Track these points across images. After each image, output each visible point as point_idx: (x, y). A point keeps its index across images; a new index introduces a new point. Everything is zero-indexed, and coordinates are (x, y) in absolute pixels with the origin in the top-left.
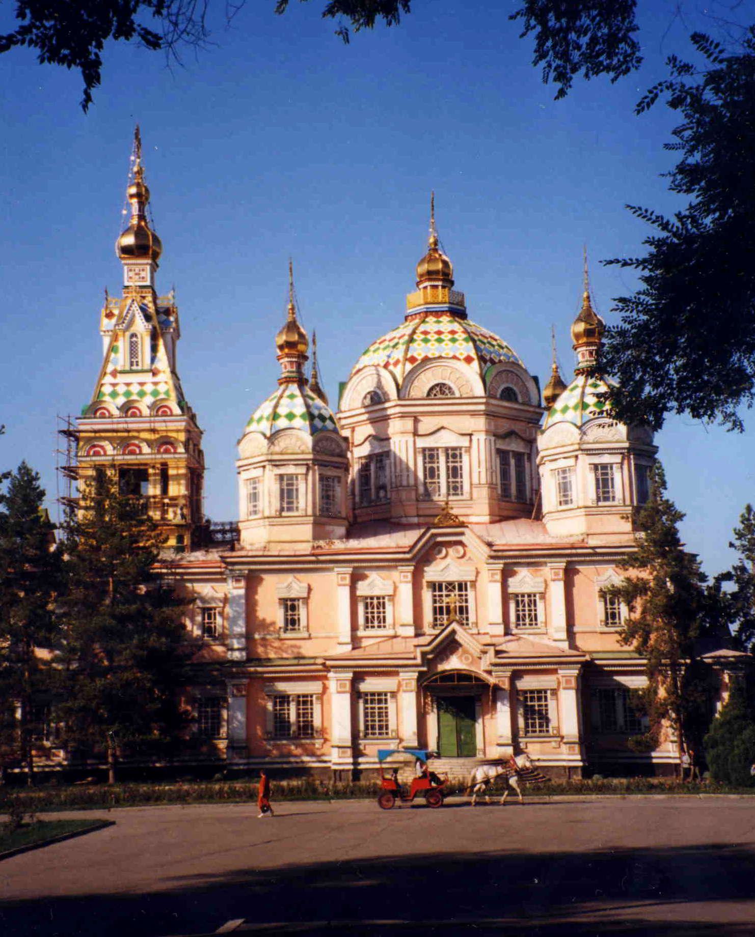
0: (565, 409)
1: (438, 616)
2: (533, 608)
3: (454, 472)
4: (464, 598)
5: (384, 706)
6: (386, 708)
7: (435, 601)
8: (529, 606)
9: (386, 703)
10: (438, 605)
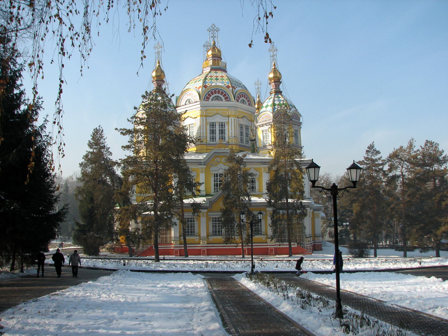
0: (267, 106)
1: (216, 187)
3: (222, 132)
5: (193, 223)
6: (194, 224)
9: (194, 222)
10: (216, 183)
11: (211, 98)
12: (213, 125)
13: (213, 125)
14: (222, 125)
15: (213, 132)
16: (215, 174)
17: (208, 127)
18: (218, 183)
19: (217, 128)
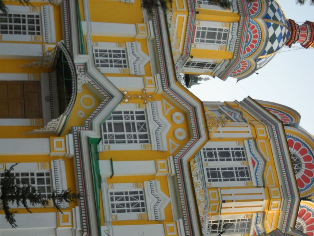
2: (131, 208)
3: (228, 174)
4: (133, 139)
7: (126, 112)
8: (133, 204)
9: (30, 33)
10: (123, 115)
11: (292, 150)
12: (240, 154)
14: (244, 174)
15: (225, 154)
16: (143, 112)
17: (233, 145)
19: (234, 164)
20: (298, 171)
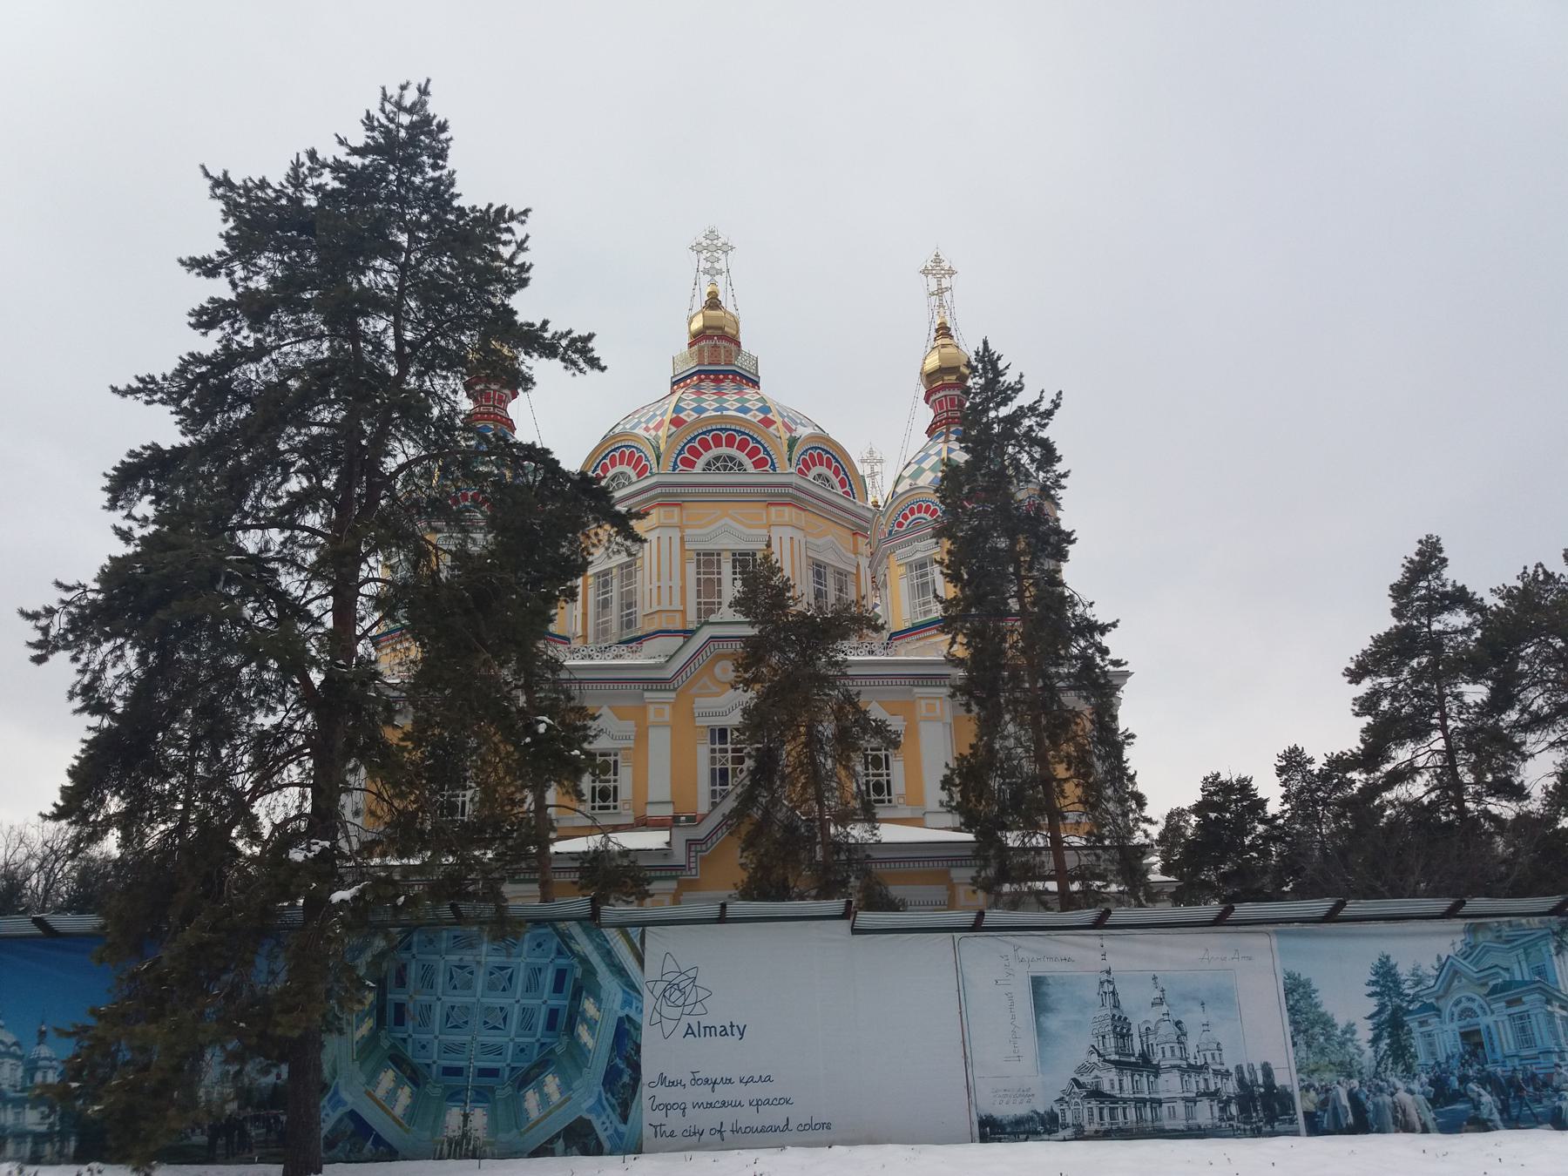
7: (713, 760)
10: (718, 767)
11: (701, 463)
13: (708, 559)
16: (713, 731)
18: (730, 766)
20: (741, 464)
